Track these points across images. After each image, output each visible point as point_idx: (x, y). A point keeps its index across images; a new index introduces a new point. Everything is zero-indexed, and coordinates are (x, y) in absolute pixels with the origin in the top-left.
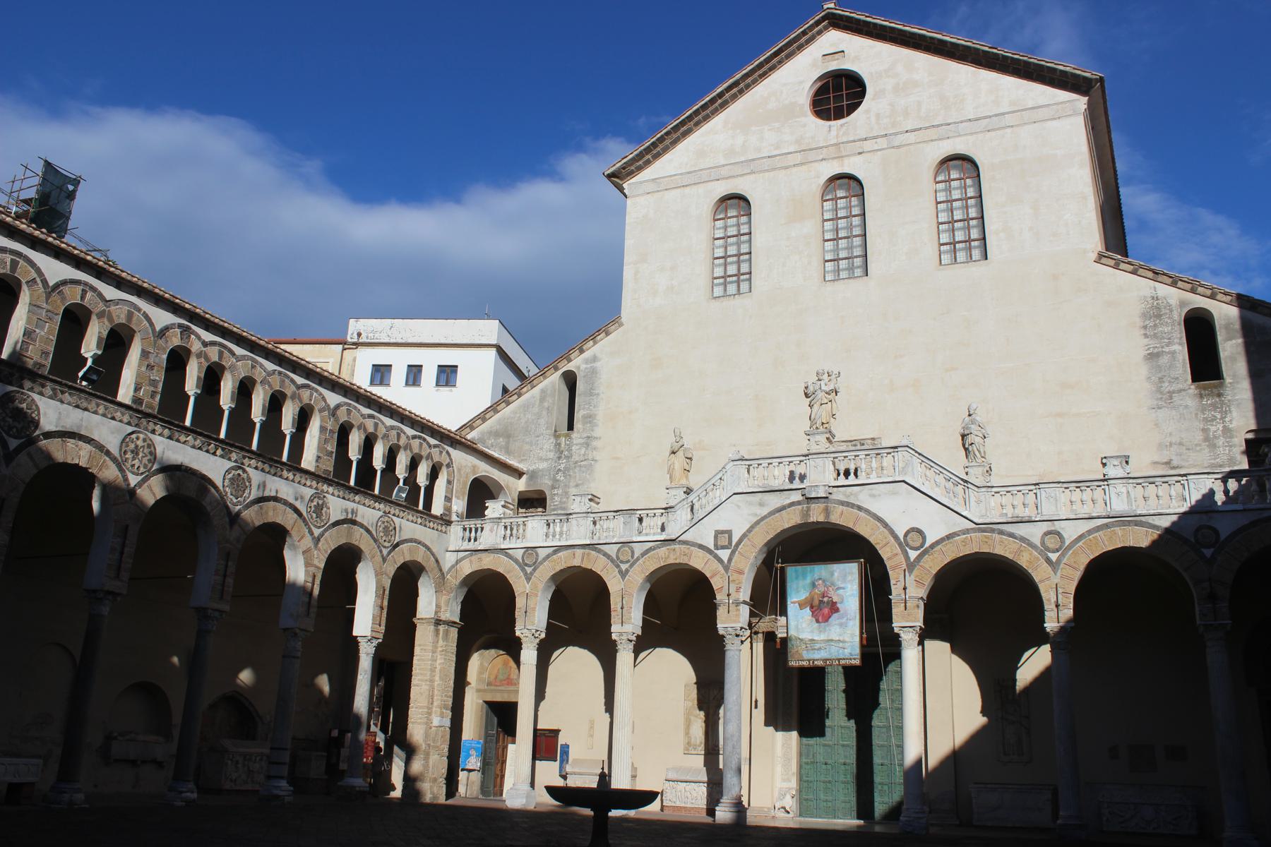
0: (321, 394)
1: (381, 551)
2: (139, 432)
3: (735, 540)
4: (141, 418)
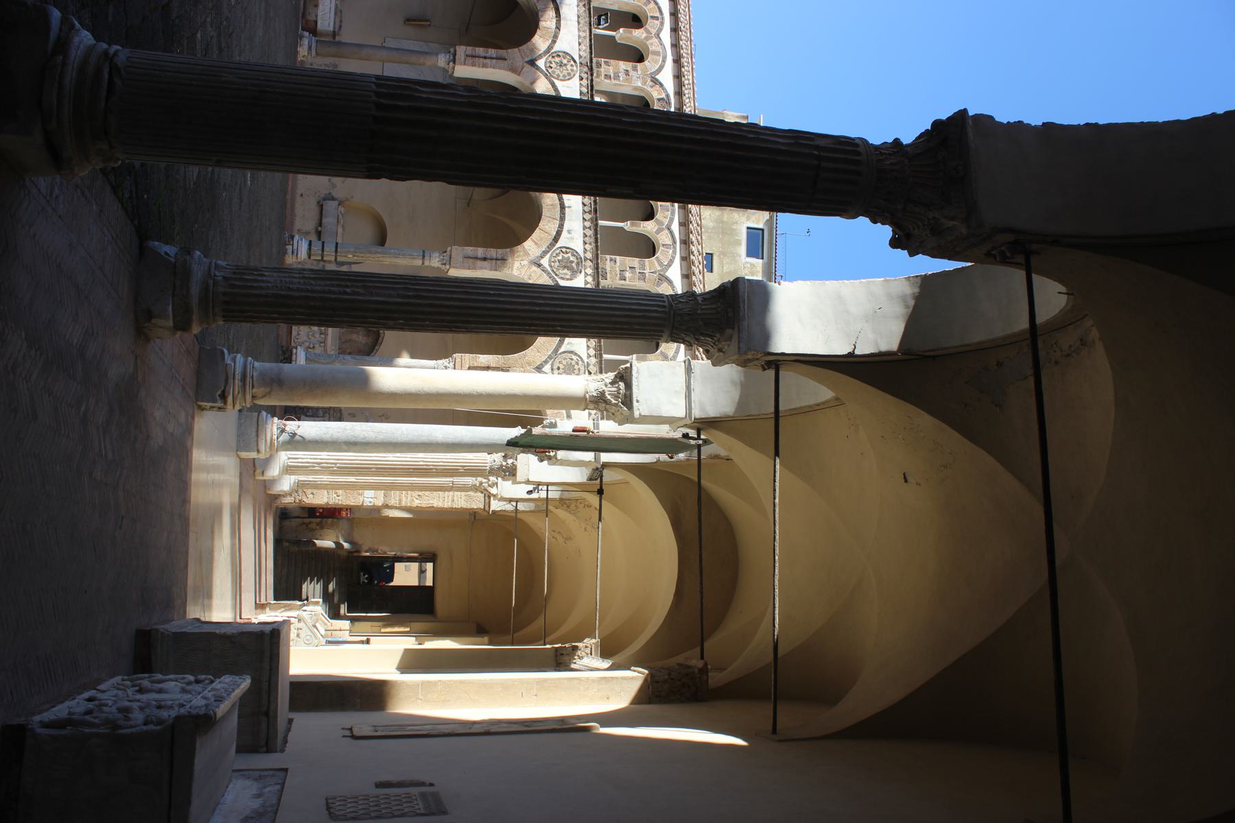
0: (674, 258)
1: (546, 362)
2: (576, 66)
4: (587, 66)
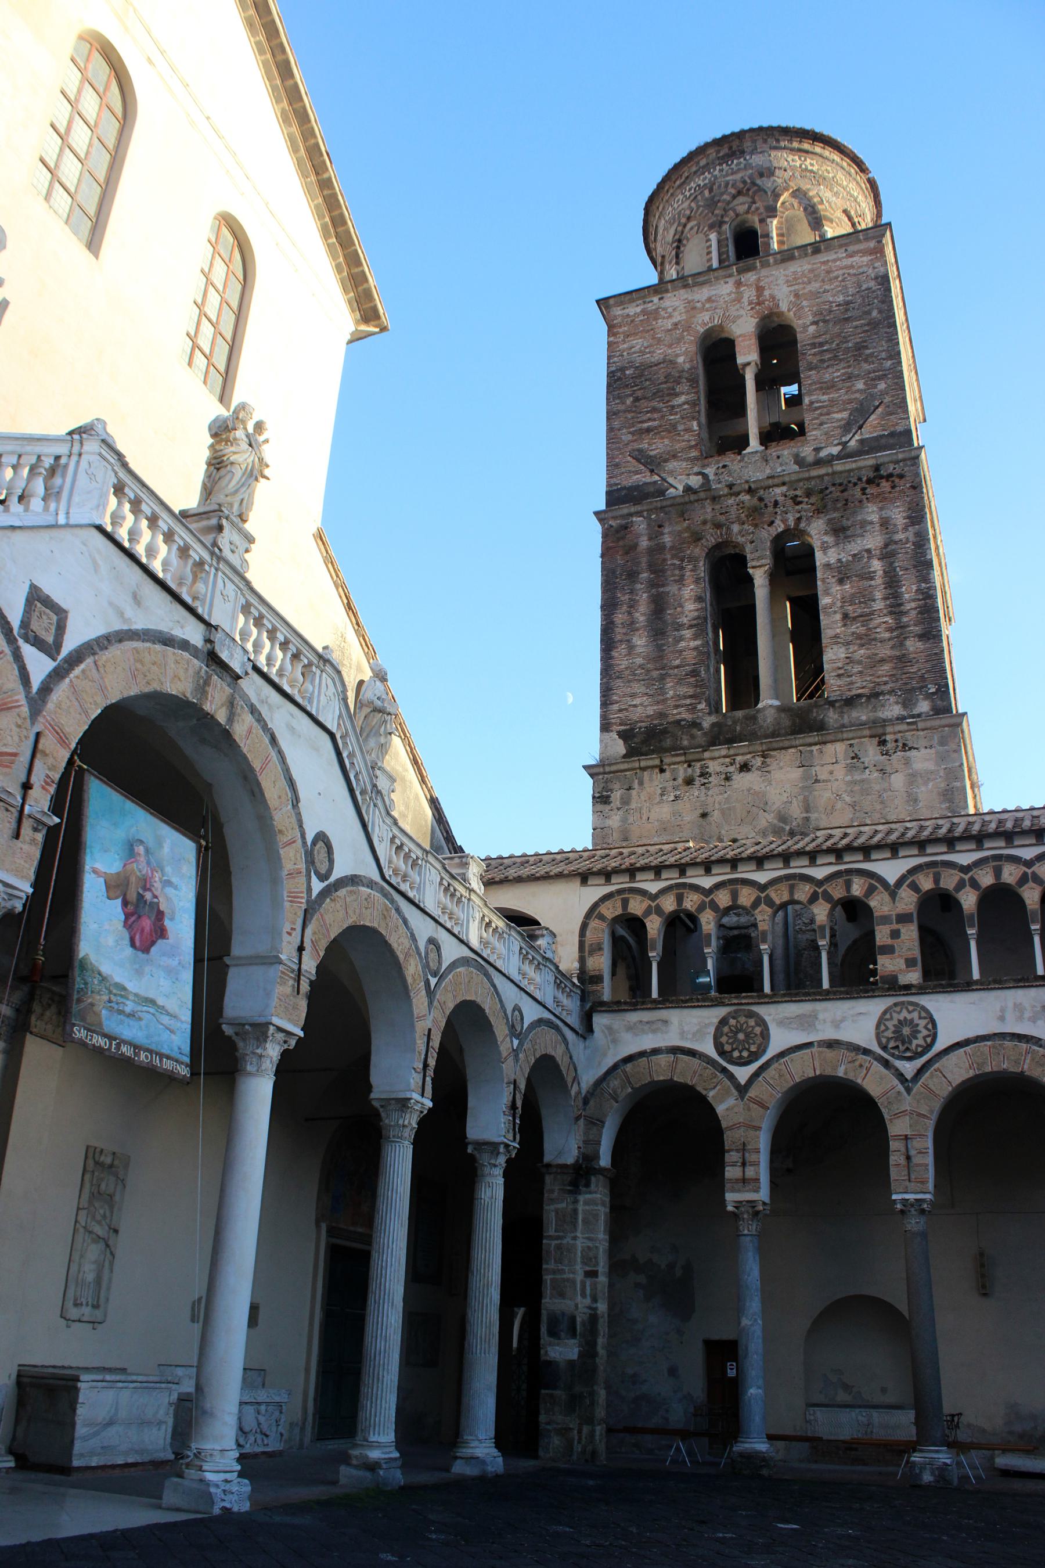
3: (70, 644)
